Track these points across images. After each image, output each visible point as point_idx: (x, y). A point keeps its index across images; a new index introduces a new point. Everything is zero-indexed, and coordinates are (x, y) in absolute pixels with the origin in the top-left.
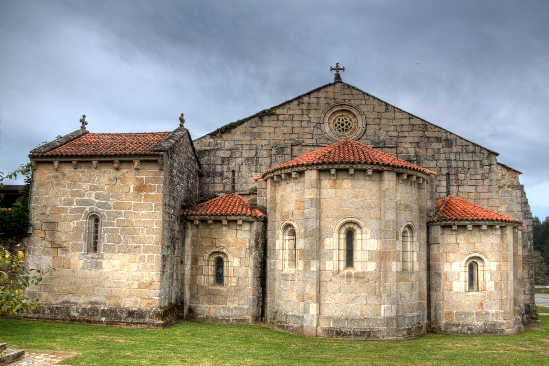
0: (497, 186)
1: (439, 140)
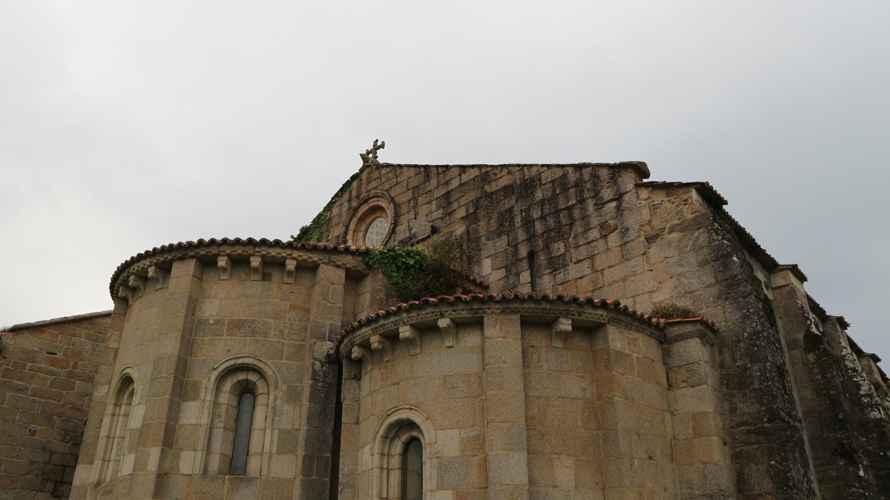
0: (643, 238)
1: (508, 190)
